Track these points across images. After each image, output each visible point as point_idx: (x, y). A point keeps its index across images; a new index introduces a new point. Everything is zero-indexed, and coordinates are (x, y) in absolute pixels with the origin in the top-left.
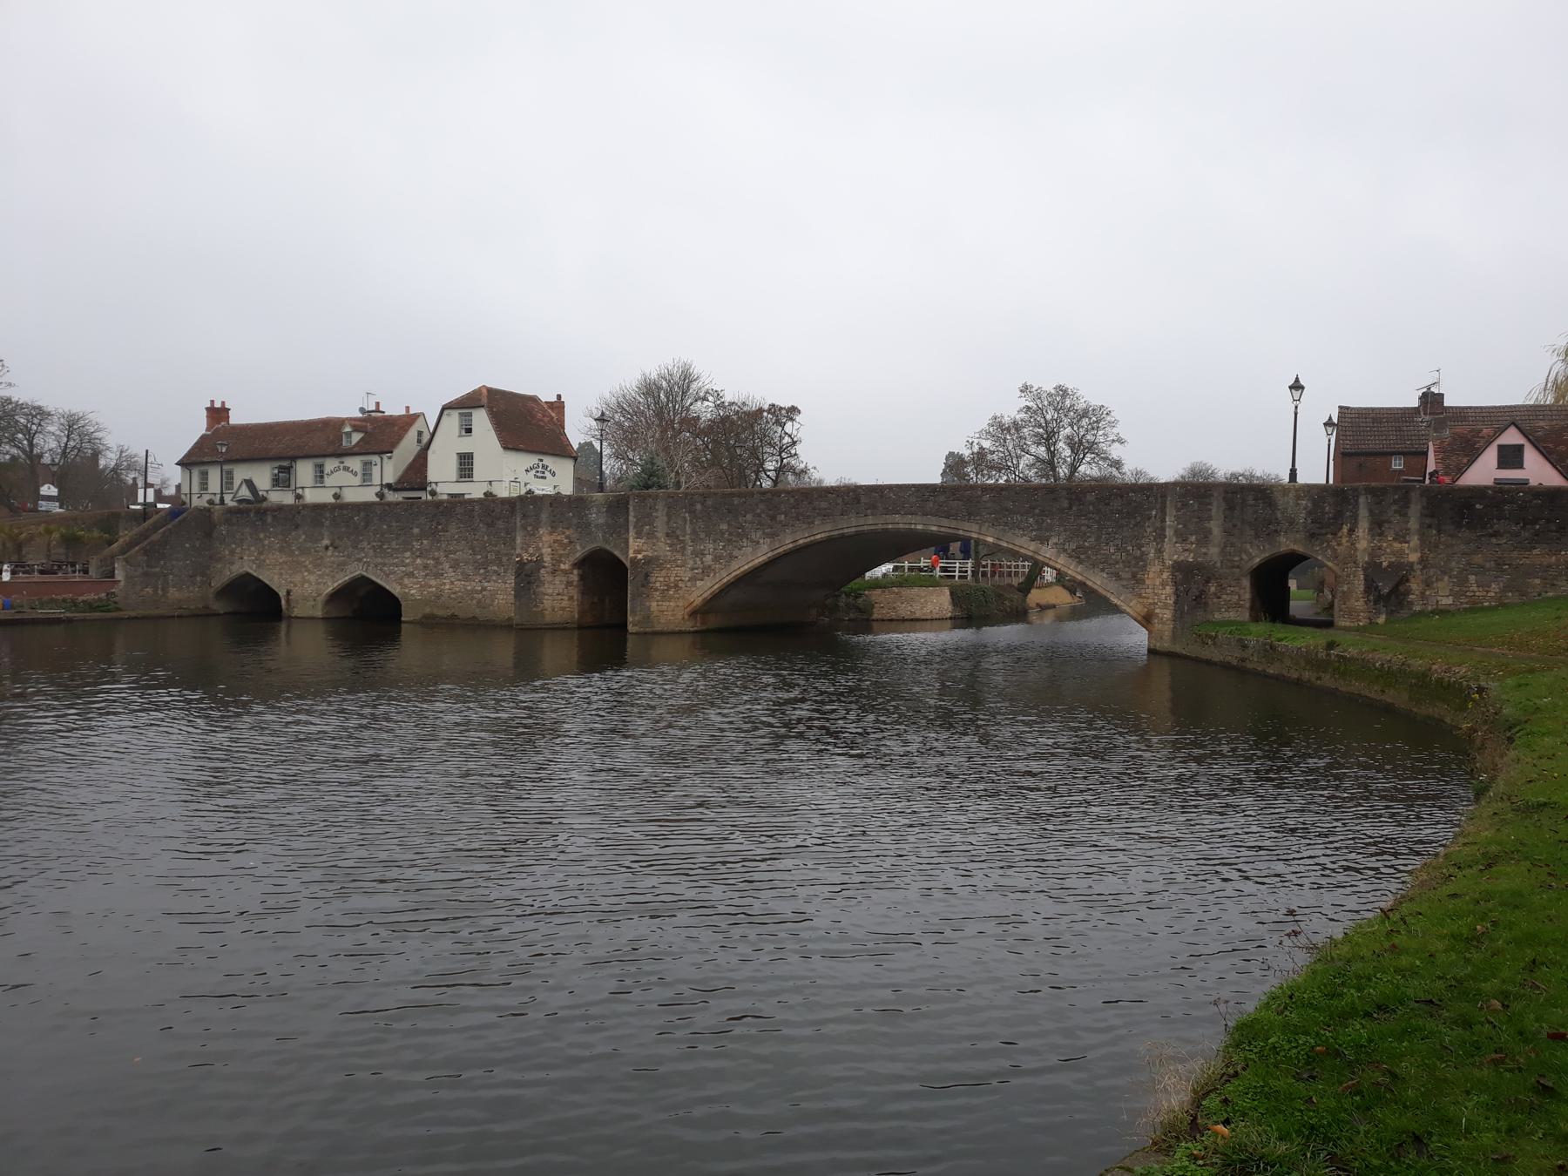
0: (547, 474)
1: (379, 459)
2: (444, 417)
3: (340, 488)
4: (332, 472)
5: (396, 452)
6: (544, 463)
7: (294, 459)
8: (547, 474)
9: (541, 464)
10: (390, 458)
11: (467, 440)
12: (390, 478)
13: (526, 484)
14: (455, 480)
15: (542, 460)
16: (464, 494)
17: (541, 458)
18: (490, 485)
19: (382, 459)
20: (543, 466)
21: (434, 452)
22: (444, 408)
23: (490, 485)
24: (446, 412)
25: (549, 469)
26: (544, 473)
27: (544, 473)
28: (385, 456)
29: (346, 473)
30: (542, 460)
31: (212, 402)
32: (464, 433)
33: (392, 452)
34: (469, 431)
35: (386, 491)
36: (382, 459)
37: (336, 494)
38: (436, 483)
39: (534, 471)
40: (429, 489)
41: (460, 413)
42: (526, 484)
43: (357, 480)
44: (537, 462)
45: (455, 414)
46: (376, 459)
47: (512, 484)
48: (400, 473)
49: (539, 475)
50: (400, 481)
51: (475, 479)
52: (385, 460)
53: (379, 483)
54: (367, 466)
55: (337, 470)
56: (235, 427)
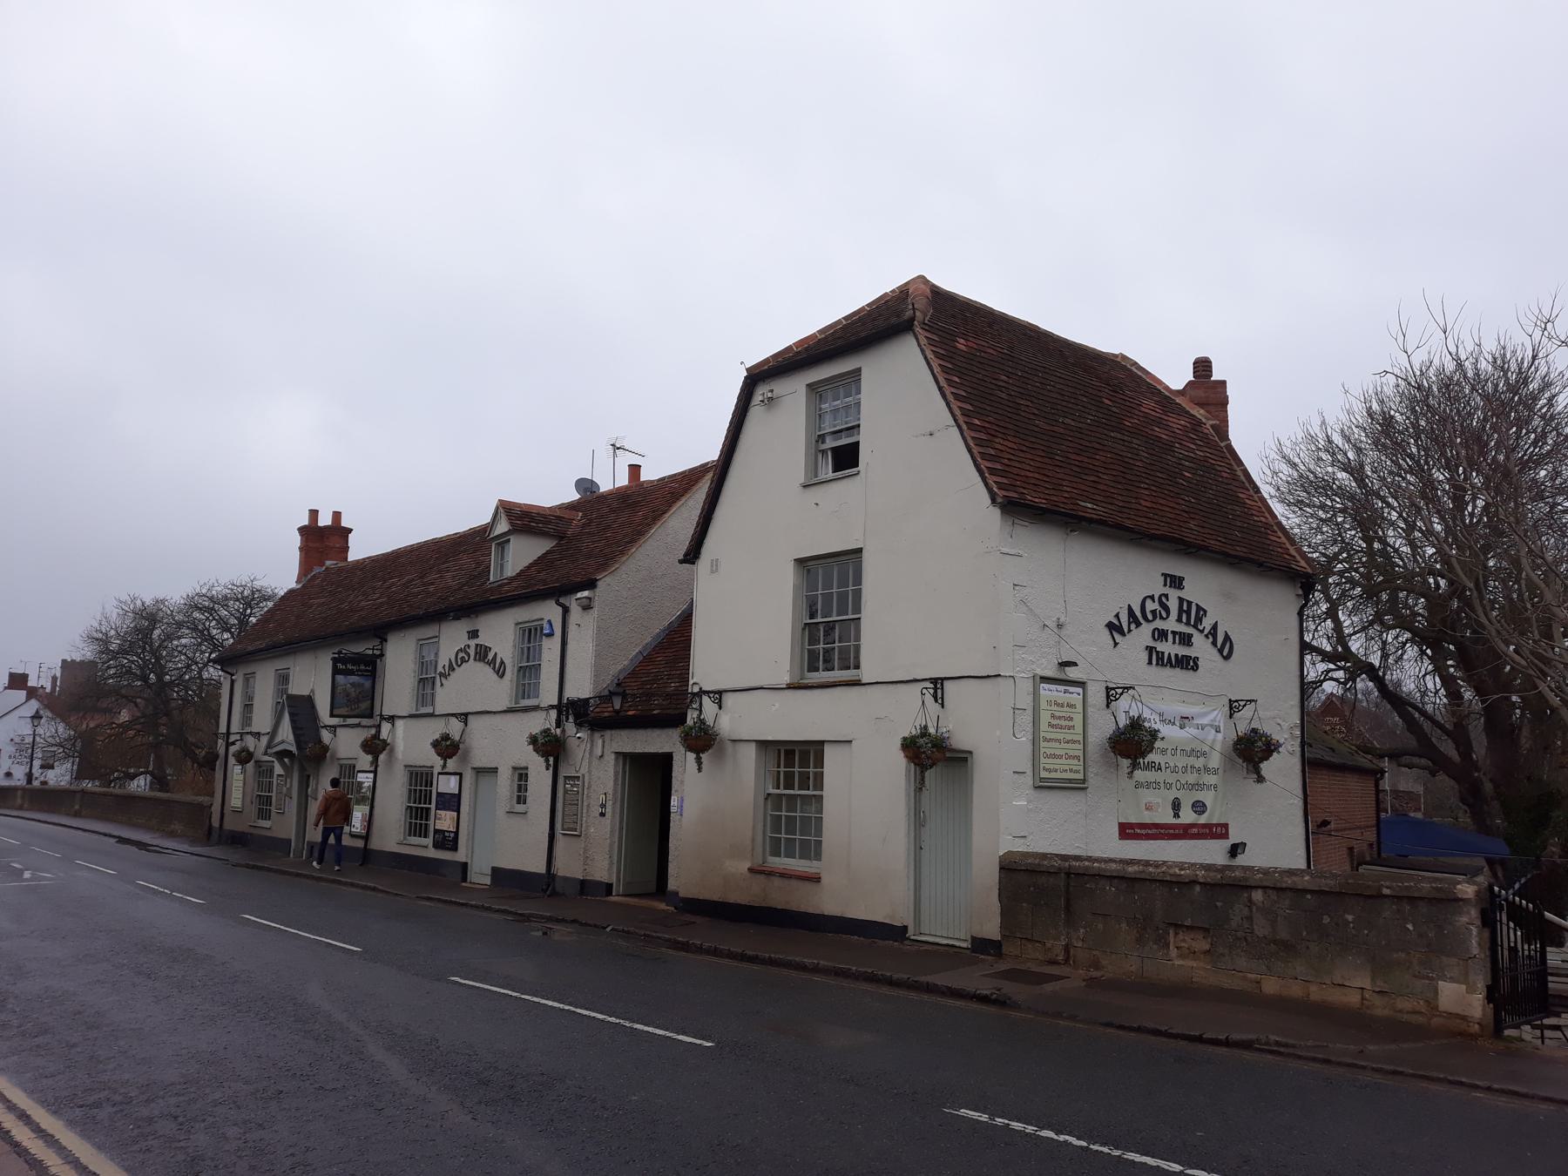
0: (1201, 647)
1: (560, 610)
2: (756, 413)
3: (464, 717)
4: (452, 668)
5: (608, 585)
6: (1182, 594)
7: (381, 631)
8: (1201, 647)
9: (1174, 595)
10: (587, 607)
11: (845, 492)
12: (581, 686)
13: (1111, 695)
14: (786, 679)
15: (1176, 582)
16: (822, 743)
17: (1177, 567)
18: (938, 697)
19: (566, 610)
20: (1185, 608)
21: (715, 566)
22: (757, 377)
23: (938, 697)
24: (761, 393)
25: (1207, 624)
26: (1186, 640)
27: (1186, 640)
28: (573, 602)
29: (480, 665)
30: (1176, 582)
31: (314, 514)
32: (827, 471)
33: (591, 584)
34: (846, 458)
35: (570, 727)
36: (566, 610)
37: (446, 737)
38: (718, 696)
39: (1146, 630)
40: (691, 717)
41: (811, 387)
42: (1111, 695)
43: (500, 692)
44: (1158, 588)
45: (793, 391)
46: (548, 611)
47: (1049, 692)
48: (621, 662)
49: (1169, 648)
50: (620, 688)
51: (866, 674)
52: (575, 610)
53: (556, 703)
54: (532, 634)
55: (461, 659)
56: (362, 565)
